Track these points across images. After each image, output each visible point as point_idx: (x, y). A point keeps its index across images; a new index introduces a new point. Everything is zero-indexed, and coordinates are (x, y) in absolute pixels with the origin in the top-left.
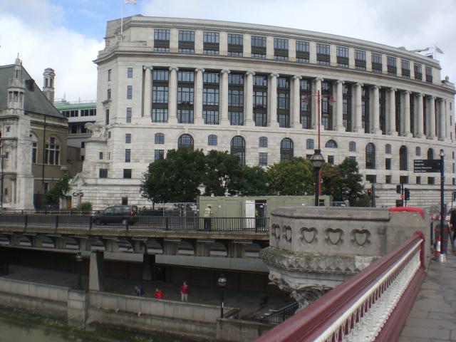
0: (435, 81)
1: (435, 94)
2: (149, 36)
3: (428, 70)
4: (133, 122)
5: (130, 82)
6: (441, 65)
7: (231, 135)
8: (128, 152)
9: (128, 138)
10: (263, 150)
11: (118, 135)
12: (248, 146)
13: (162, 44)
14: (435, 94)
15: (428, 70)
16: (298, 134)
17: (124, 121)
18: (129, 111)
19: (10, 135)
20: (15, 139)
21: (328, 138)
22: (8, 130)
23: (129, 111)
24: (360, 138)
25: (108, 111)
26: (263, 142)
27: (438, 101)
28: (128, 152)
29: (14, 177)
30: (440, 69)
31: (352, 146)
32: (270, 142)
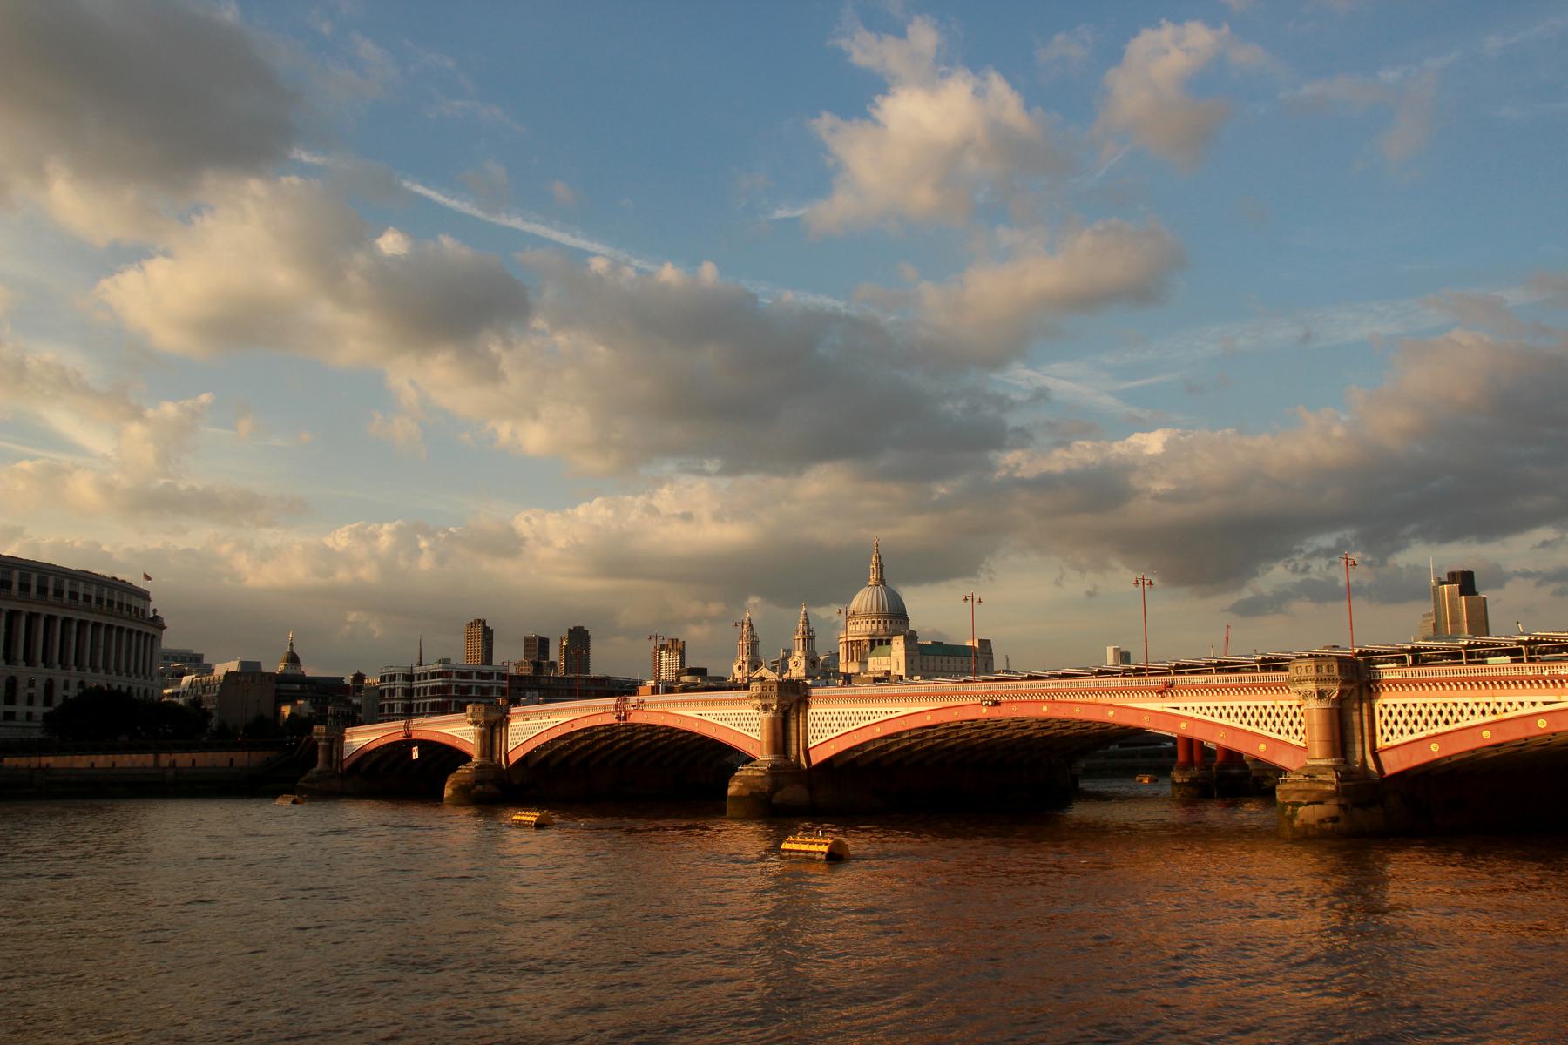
6: (151, 595)
10: (31, 691)
14: (151, 631)
21: (79, 679)
30: (149, 600)
32: (37, 684)
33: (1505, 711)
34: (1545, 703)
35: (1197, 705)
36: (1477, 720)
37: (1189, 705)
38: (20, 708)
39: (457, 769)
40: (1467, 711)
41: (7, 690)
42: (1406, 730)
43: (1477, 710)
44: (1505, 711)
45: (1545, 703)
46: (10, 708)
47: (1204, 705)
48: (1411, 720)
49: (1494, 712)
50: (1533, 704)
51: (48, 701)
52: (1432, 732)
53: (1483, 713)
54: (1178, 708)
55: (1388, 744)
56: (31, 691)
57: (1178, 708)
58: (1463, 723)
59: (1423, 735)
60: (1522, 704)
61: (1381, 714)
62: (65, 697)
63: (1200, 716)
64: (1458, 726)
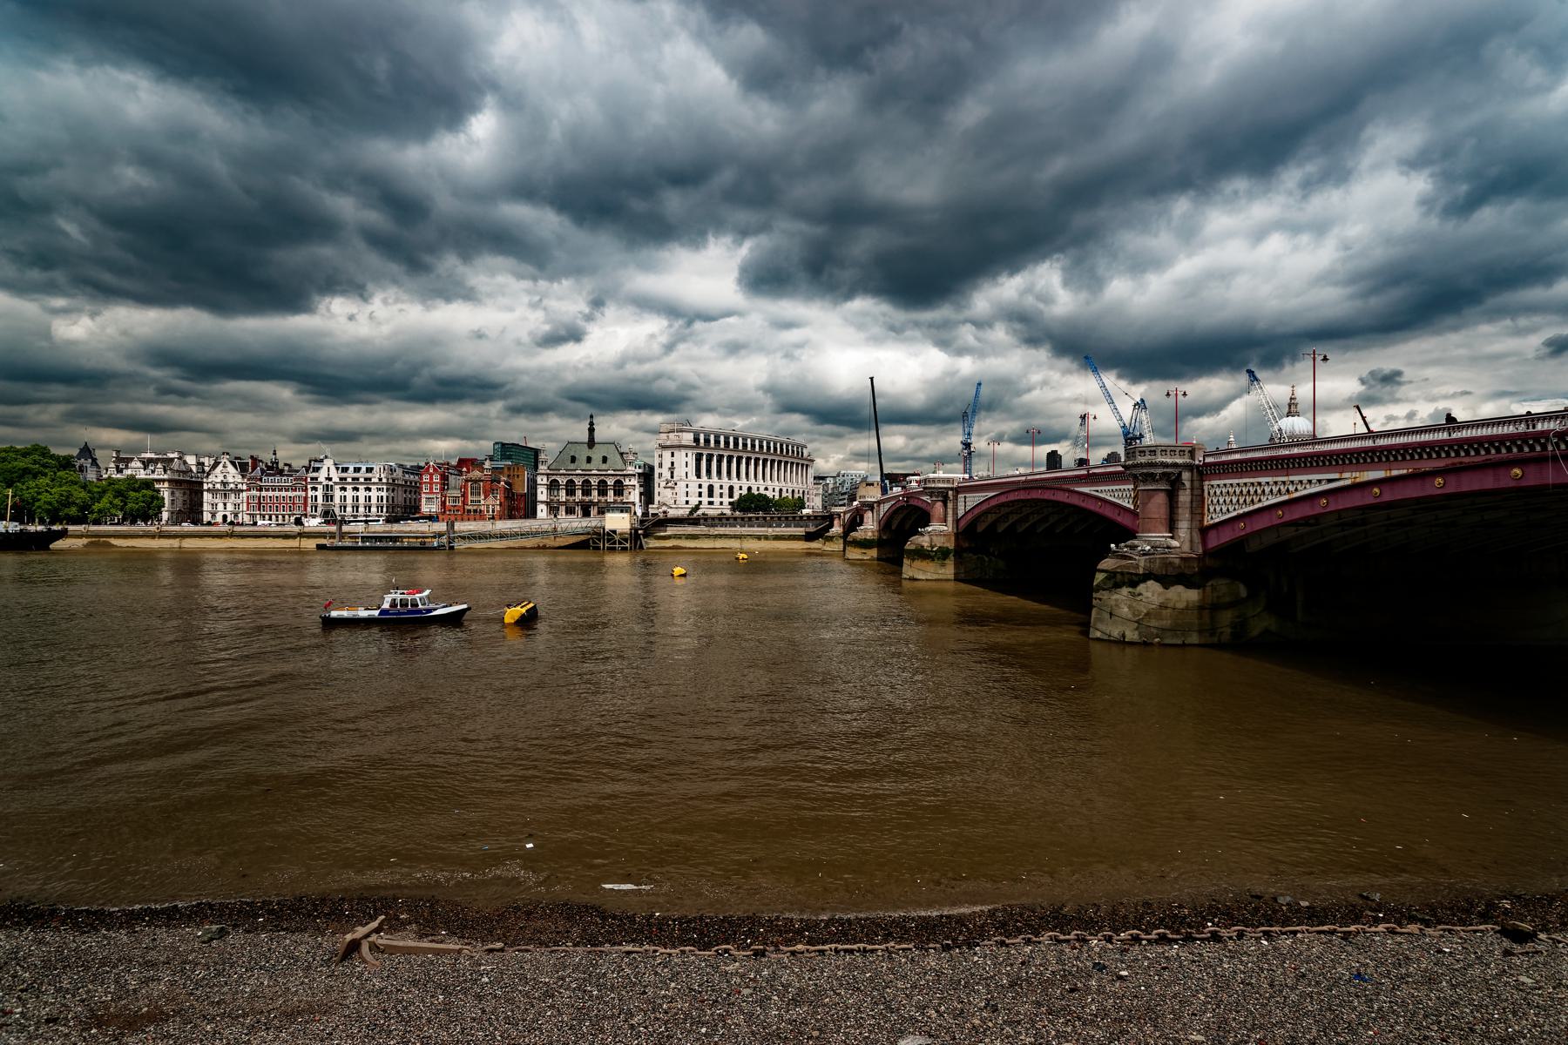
0: (805, 455)
1: (806, 463)
2: (691, 436)
3: (802, 449)
5: (687, 459)
11: (681, 485)
13: (697, 440)
14: (806, 463)
15: (802, 449)
17: (685, 478)
19: (631, 483)
24: (777, 485)
25: (672, 473)
26: (721, 487)
27: (807, 466)
29: (633, 503)
31: (774, 491)
33: (1296, 490)
34: (1330, 481)
35: (1107, 488)
37: (1103, 488)
41: (713, 491)
42: (1224, 509)
43: (1275, 489)
44: (1296, 490)
45: (1330, 481)
47: (1111, 488)
48: (1228, 500)
49: (1288, 491)
50: (1320, 481)
51: (731, 496)
52: (1241, 511)
54: (1097, 491)
55: (1212, 522)
57: (1097, 491)
59: (1234, 514)
60: (1310, 482)
61: (1209, 493)
62: (741, 494)
64: (1260, 505)
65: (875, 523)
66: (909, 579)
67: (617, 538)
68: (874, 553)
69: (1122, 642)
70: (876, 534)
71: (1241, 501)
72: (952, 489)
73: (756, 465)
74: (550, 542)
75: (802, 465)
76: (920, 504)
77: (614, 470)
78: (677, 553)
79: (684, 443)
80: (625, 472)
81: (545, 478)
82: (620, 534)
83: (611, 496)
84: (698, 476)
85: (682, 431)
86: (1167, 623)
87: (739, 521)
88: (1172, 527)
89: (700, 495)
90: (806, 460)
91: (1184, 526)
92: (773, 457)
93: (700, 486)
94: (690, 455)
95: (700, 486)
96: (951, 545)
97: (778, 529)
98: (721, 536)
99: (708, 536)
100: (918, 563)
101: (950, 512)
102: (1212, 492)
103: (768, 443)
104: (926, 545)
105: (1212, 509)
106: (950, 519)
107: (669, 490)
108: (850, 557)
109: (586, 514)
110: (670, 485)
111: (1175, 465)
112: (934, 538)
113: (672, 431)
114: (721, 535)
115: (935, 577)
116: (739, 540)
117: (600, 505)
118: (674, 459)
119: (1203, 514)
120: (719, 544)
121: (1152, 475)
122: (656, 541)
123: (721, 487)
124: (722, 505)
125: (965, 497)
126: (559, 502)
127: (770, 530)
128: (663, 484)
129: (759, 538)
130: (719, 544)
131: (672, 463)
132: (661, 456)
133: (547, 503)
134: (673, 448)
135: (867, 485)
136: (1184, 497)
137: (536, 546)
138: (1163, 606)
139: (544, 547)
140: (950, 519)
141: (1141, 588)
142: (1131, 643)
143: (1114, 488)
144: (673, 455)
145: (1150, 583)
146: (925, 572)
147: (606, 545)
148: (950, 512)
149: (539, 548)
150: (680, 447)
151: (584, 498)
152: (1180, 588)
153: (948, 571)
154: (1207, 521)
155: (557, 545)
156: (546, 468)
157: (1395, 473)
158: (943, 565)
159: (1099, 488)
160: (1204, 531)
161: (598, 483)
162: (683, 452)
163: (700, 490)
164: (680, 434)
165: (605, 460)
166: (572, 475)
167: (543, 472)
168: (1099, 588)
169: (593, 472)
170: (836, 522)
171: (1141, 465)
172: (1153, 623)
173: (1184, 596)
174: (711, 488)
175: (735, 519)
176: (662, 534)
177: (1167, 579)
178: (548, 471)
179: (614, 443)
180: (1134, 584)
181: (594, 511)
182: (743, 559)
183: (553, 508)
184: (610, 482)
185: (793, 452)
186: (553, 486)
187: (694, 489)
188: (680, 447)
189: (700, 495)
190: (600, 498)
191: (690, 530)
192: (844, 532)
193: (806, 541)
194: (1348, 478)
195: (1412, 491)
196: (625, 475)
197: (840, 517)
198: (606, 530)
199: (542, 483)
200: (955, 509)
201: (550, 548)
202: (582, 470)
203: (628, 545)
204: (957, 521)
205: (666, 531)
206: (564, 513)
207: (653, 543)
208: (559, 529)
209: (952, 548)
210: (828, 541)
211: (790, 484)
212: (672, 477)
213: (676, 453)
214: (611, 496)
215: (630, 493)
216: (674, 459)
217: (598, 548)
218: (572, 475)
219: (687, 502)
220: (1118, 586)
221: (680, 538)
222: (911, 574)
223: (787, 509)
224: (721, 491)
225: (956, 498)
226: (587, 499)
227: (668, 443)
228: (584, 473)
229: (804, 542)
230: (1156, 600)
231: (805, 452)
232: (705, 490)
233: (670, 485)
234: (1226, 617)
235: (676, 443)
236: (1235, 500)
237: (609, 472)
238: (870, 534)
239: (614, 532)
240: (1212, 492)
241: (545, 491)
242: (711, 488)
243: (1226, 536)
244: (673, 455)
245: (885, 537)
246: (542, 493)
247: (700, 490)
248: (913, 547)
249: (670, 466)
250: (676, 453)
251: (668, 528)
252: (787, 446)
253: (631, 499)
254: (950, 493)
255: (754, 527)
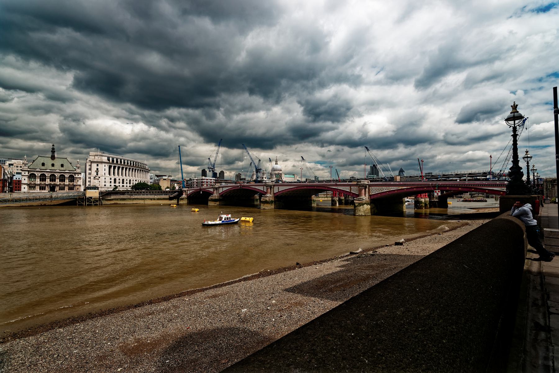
0: (147, 168)
1: (148, 171)
2: (106, 158)
4: (106, 176)
5: (105, 168)
7: (122, 179)
8: (105, 181)
9: (105, 178)
12: (124, 181)
13: (109, 160)
16: (131, 178)
18: (105, 173)
19: (78, 177)
20: (80, 178)
22: (78, 175)
23: (105, 173)
27: (148, 172)
28: (105, 181)
29: (80, 185)
34: (397, 188)
36: (386, 191)
38: (125, 185)
39: (210, 196)
40: (385, 189)
42: (375, 192)
43: (386, 189)
45: (397, 188)
46: (123, 185)
47: (342, 187)
48: (376, 190)
51: (130, 184)
53: (387, 189)
56: (127, 181)
58: (384, 191)
63: (342, 189)
65: (218, 194)
66: (263, 209)
67: (92, 200)
68: (218, 203)
69: (362, 215)
70: (219, 197)
71: (379, 191)
72: (273, 185)
73: (132, 171)
74: (48, 202)
75: (147, 172)
76: (250, 188)
77: (69, 171)
78: (117, 206)
79: (104, 161)
80: (75, 172)
81: (27, 173)
82: (94, 199)
83: (67, 182)
84: (110, 174)
85: (102, 156)
86: (367, 212)
87: (145, 193)
88: (365, 195)
89: (111, 182)
90: (147, 169)
91: (367, 195)
92: (136, 168)
93: (111, 179)
94: (106, 166)
95: (111, 179)
96: (273, 200)
97: (159, 196)
98: (135, 199)
99: (130, 199)
100: (266, 205)
101: (272, 191)
102: (372, 189)
103: (131, 162)
104: (268, 200)
105: (372, 192)
106: (272, 193)
107: (97, 180)
108: (210, 205)
109: (52, 189)
110: (97, 178)
111: (366, 184)
112: (270, 198)
113: (97, 156)
114: (135, 198)
115: (270, 208)
116: (143, 200)
117: (70, 186)
118: (98, 167)
119: (370, 193)
120: (135, 202)
121: (363, 186)
122: (106, 201)
123: (119, 179)
124: (127, 187)
125: (278, 188)
126: (36, 185)
127: (156, 196)
128: (92, 178)
129: (151, 199)
130: (135, 202)
131: (97, 169)
132: (91, 165)
133: (28, 185)
134: (98, 163)
135: (164, 180)
136: (367, 190)
137: (40, 205)
138: (367, 209)
139: (45, 205)
140: (272, 193)
141: (364, 205)
142: (363, 216)
143: (344, 187)
144: (98, 165)
145: (365, 205)
146: (268, 207)
147: (87, 203)
148: (272, 191)
149: (41, 205)
150: (102, 162)
151: (51, 182)
152: (368, 205)
153: (273, 207)
154: (371, 194)
155: (52, 204)
156: (27, 168)
157: (408, 187)
158: (272, 205)
159: (339, 187)
160: (370, 196)
161: (60, 176)
162: (103, 165)
163: (111, 180)
164: (101, 157)
165: (62, 166)
166: (44, 172)
167: (26, 169)
168: (357, 206)
169: (57, 171)
170: (184, 193)
171: (362, 184)
172: (366, 212)
173: (369, 207)
174: (115, 180)
175: (134, 192)
176: (109, 198)
177: (367, 204)
178: (29, 169)
179: (66, 158)
180: (363, 205)
181: (57, 188)
182: (175, 206)
183: (31, 186)
184: (67, 176)
185: (140, 166)
186: (32, 176)
187: (108, 180)
188: (102, 162)
189: (111, 182)
190: (61, 183)
191: (122, 197)
192: (187, 197)
193: (169, 200)
194: (400, 188)
195: (411, 190)
196: (75, 173)
197: (185, 191)
198: (87, 197)
199: (25, 175)
200: (273, 191)
201: (48, 205)
202: (50, 170)
203: (98, 203)
204: (274, 194)
205: (111, 197)
206: (38, 189)
207: (104, 202)
208: (53, 197)
209: (273, 200)
210: (182, 200)
211: (134, 178)
212: (97, 174)
213: (99, 165)
214: (67, 182)
215: (78, 181)
216: (98, 167)
217: (82, 205)
218: (44, 172)
219: (105, 185)
220: (360, 205)
221: (117, 200)
222: (264, 208)
223: (155, 188)
224: (119, 181)
225: (273, 188)
226: (53, 183)
227: (95, 160)
228: (51, 171)
229: (168, 201)
230: (366, 208)
231: (147, 166)
232: (113, 181)
233: (97, 178)
234: (373, 210)
235: (99, 160)
236: (377, 190)
237: (66, 171)
238: (217, 197)
239: (91, 198)
240: (372, 189)
241: (26, 179)
242: (115, 180)
243: (375, 197)
244: (98, 165)
245: (221, 198)
246: (25, 179)
247: (111, 180)
248: (264, 200)
249: (96, 170)
250: (99, 165)
251: (112, 196)
252: (138, 163)
253: (79, 183)
254: (272, 186)
255: (148, 195)
